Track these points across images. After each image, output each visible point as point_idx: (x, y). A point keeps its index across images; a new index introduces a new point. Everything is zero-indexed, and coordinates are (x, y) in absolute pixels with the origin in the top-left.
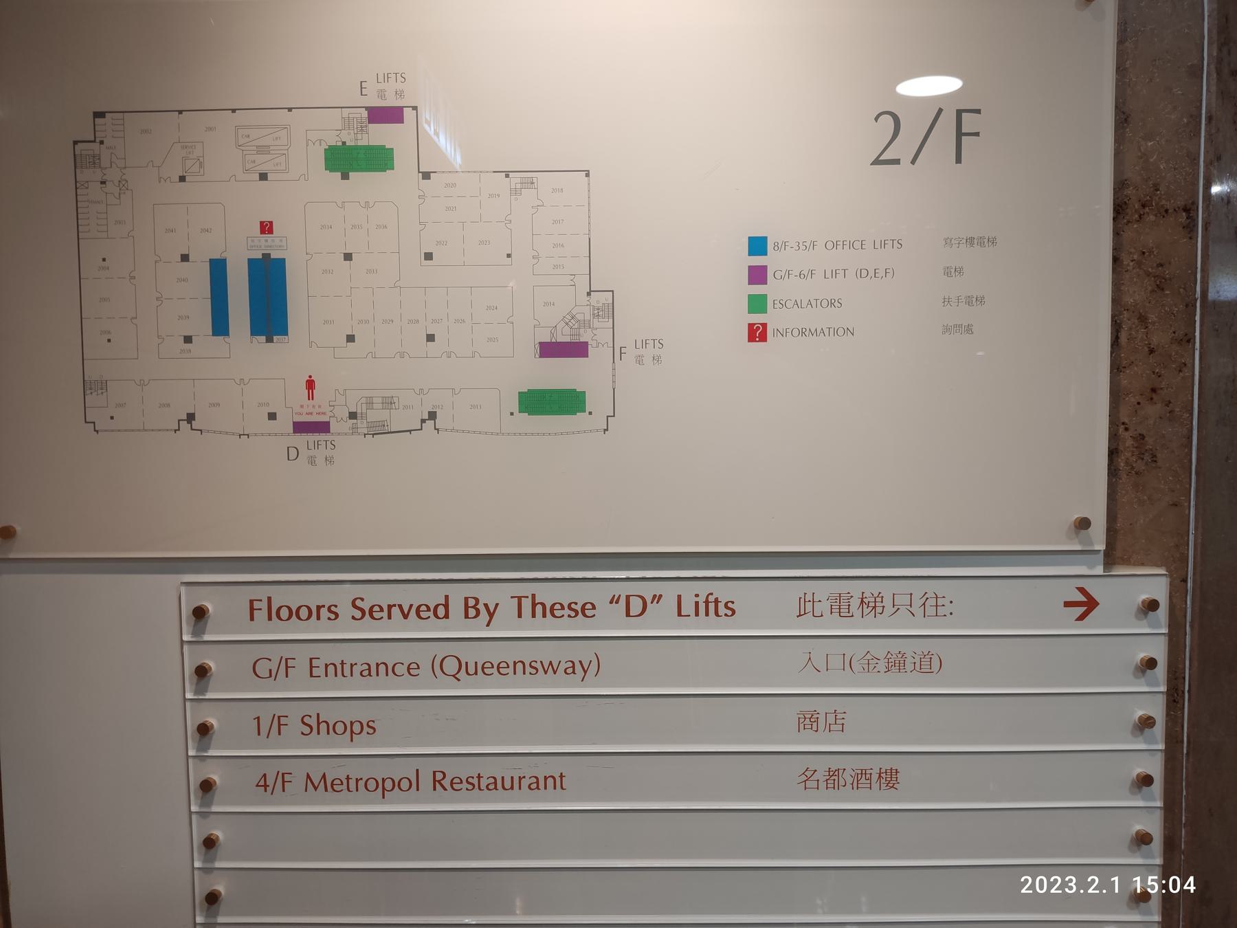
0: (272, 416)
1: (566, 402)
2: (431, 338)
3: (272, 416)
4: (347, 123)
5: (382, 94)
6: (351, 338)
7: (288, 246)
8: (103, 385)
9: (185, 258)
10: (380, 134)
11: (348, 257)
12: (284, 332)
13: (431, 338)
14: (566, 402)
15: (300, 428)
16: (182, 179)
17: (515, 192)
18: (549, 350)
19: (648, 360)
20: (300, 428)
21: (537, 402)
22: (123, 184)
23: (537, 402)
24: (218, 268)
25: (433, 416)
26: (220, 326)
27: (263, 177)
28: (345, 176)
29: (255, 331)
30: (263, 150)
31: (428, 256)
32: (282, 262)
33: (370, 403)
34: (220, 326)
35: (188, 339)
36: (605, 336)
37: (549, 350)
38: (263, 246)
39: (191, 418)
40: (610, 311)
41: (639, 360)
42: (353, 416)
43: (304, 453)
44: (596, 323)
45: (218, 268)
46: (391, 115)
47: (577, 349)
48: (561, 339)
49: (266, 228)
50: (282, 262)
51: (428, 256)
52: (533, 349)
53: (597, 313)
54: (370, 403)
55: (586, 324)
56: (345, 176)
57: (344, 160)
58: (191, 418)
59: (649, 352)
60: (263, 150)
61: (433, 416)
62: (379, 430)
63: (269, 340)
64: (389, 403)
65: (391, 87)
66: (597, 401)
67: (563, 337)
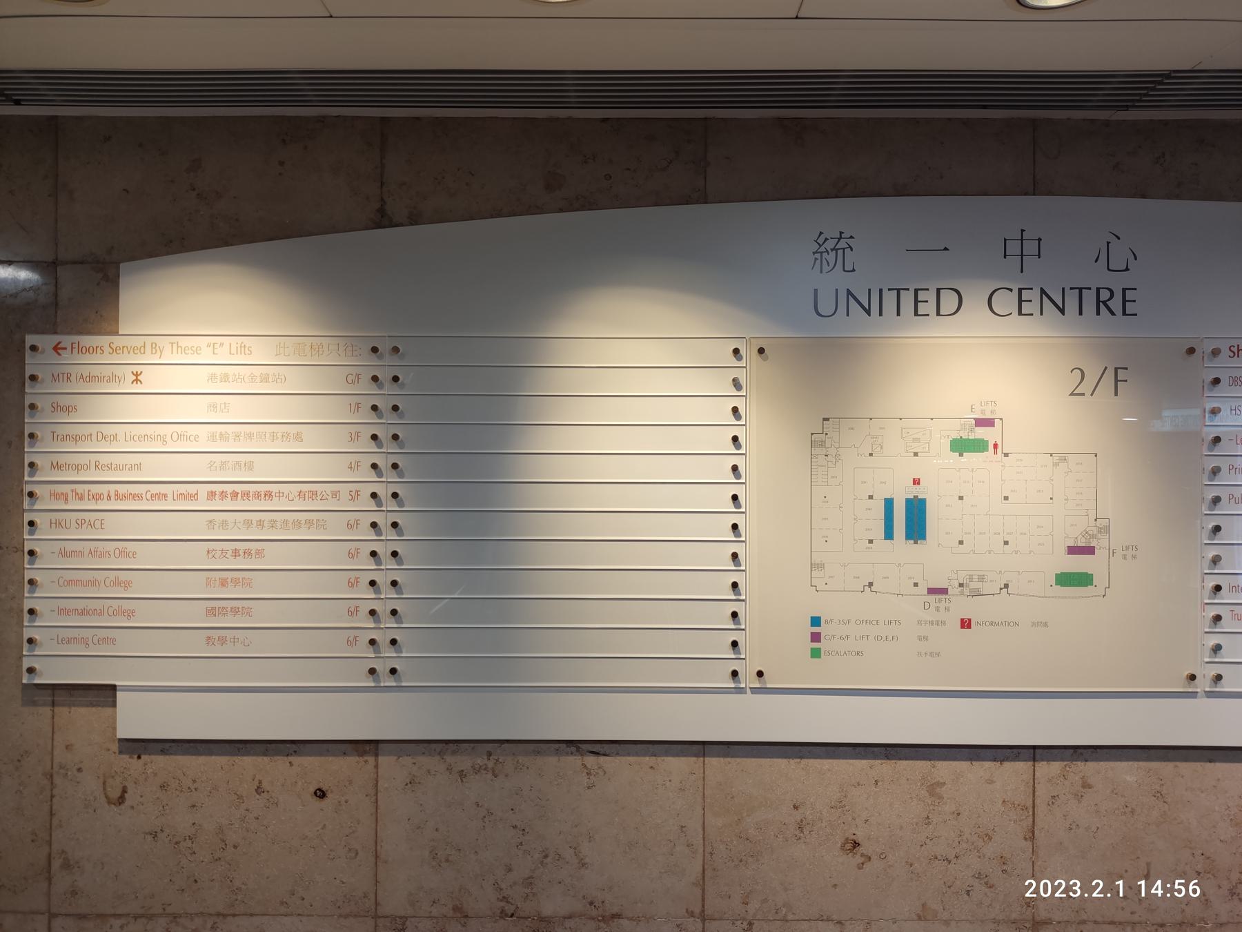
0: (916, 585)
1: (1083, 580)
2: (1006, 543)
3: (916, 585)
4: (963, 427)
5: (983, 412)
6: (961, 542)
7: (926, 491)
8: (821, 566)
9: (871, 497)
10: (981, 433)
11: (961, 498)
12: (924, 538)
13: (1006, 543)
14: (1083, 580)
15: (932, 591)
16: (871, 455)
17: (1056, 464)
18: (1073, 550)
19: (1129, 557)
20: (932, 591)
21: (1065, 579)
22: (837, 457)
23: (1065, 579)
24: (889, 503)
25: (1006, 586)
26: (889, 534)
27: (916, 454)
28: (961, 455)
29: (908, 537)
30: (916, 440)
31: (1006, 498)
32: (924, 501)
33: (971, 578)
34: (889, 534)
35: (871, 542)
36: (1104, 543)
37: (1073, 550)
38: (913, 491)
39: (871, 584)
40: (1106, 530)
41: (1124, 557)
42: (961, 585)
43: (933, 605)
44: (1099, 536)
45: (889, 503)
46: (989, 423)
47: (1090, 550)
48: (1080, 544)
49: (916, 482)
50: (924, 501)
51: (1006, 498)
52: (1063, 550)
53: (1100, 530)
54: (971, 578)
55: (1094, 536)
56: (961, 455)
57: (961, 446)
58: (871, 584)
59: (1130, 553)
60: (916, 440)
61: (1006, 586)
62: (976, 593)
63: (916, 543)
64: (982, 579)
65: (988, 409)
66: (1100, 579)
67: (1081, 543)
